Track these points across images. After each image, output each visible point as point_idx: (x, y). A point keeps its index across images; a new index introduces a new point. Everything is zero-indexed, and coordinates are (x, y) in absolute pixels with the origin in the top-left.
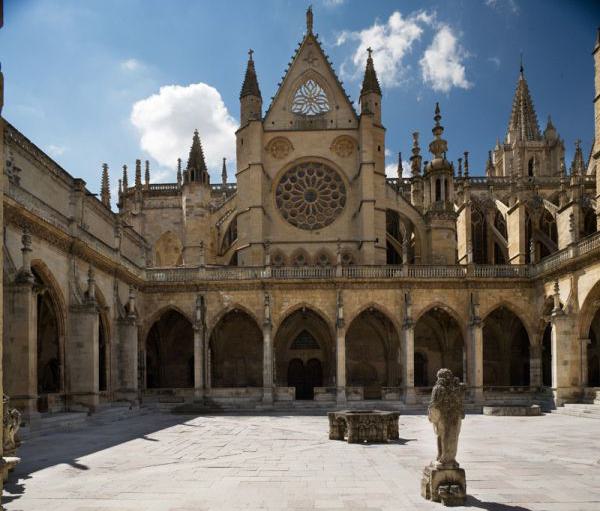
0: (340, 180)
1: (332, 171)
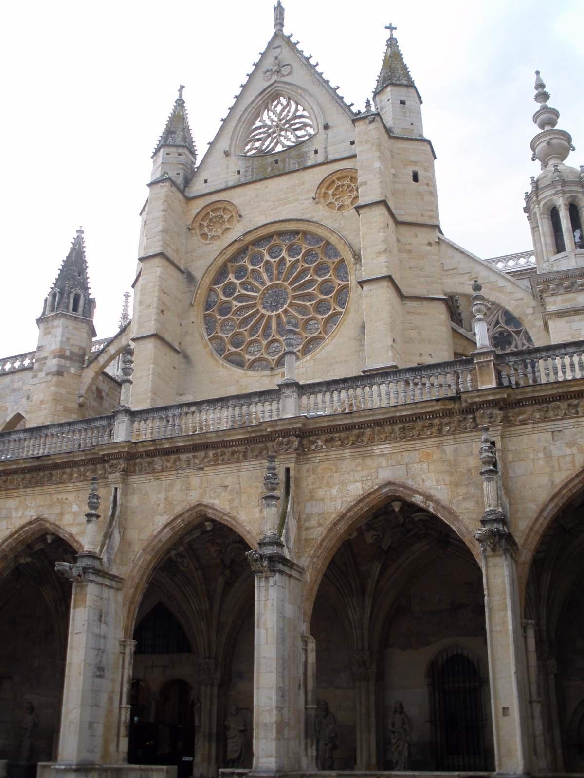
0: (337, 254)
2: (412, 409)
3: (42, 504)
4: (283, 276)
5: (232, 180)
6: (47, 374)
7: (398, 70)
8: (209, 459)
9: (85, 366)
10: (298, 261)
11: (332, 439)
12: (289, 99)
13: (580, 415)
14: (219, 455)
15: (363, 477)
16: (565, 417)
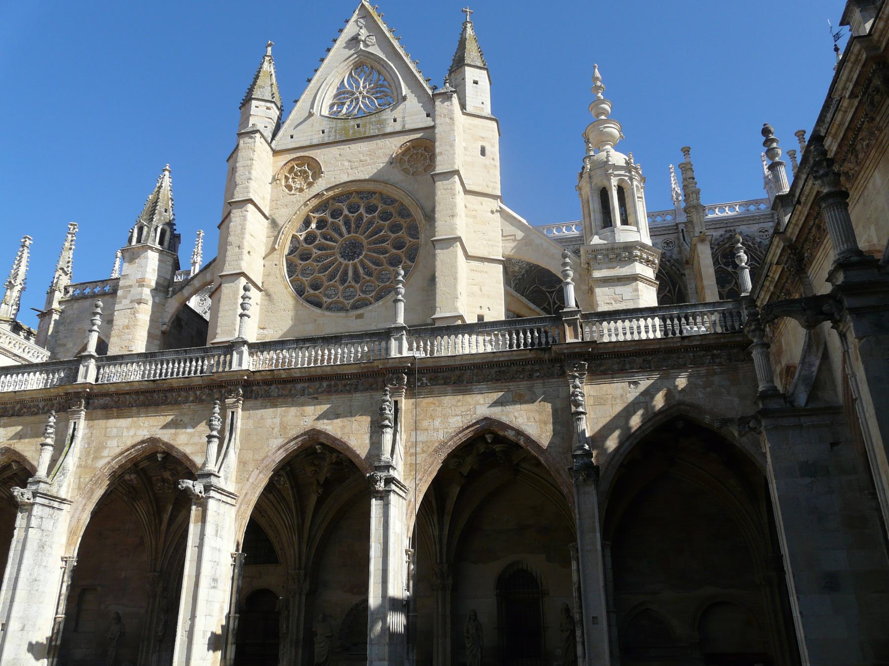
0: (409, 215)
1: (393, 201)
3: (155, 424)
4: (360, 229)
5: (316, 139)
6: (132, 302)
8: (323, 389)
9: (169, 296)
10: (374, 217)
12: (372, 68)
13: (653, 369)
14: (332, 387)
15: (462, 412)
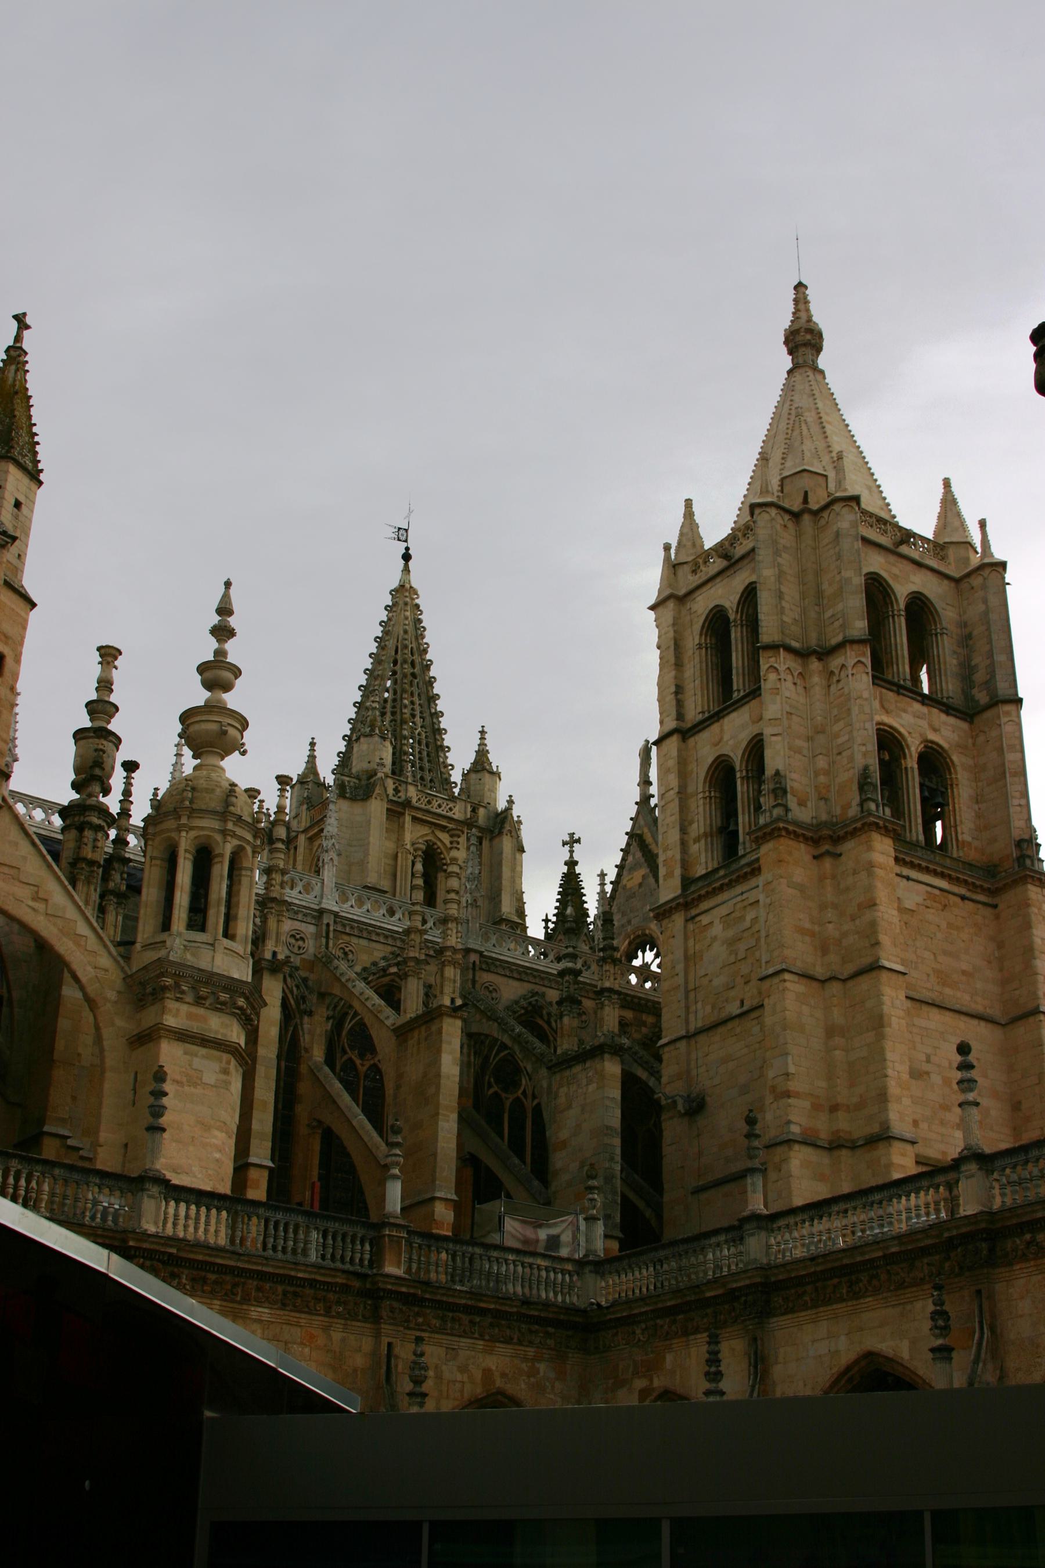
2: (310, 1273)
7: (22, 428)
11: (205, 1280)
16: (464, 1335)
